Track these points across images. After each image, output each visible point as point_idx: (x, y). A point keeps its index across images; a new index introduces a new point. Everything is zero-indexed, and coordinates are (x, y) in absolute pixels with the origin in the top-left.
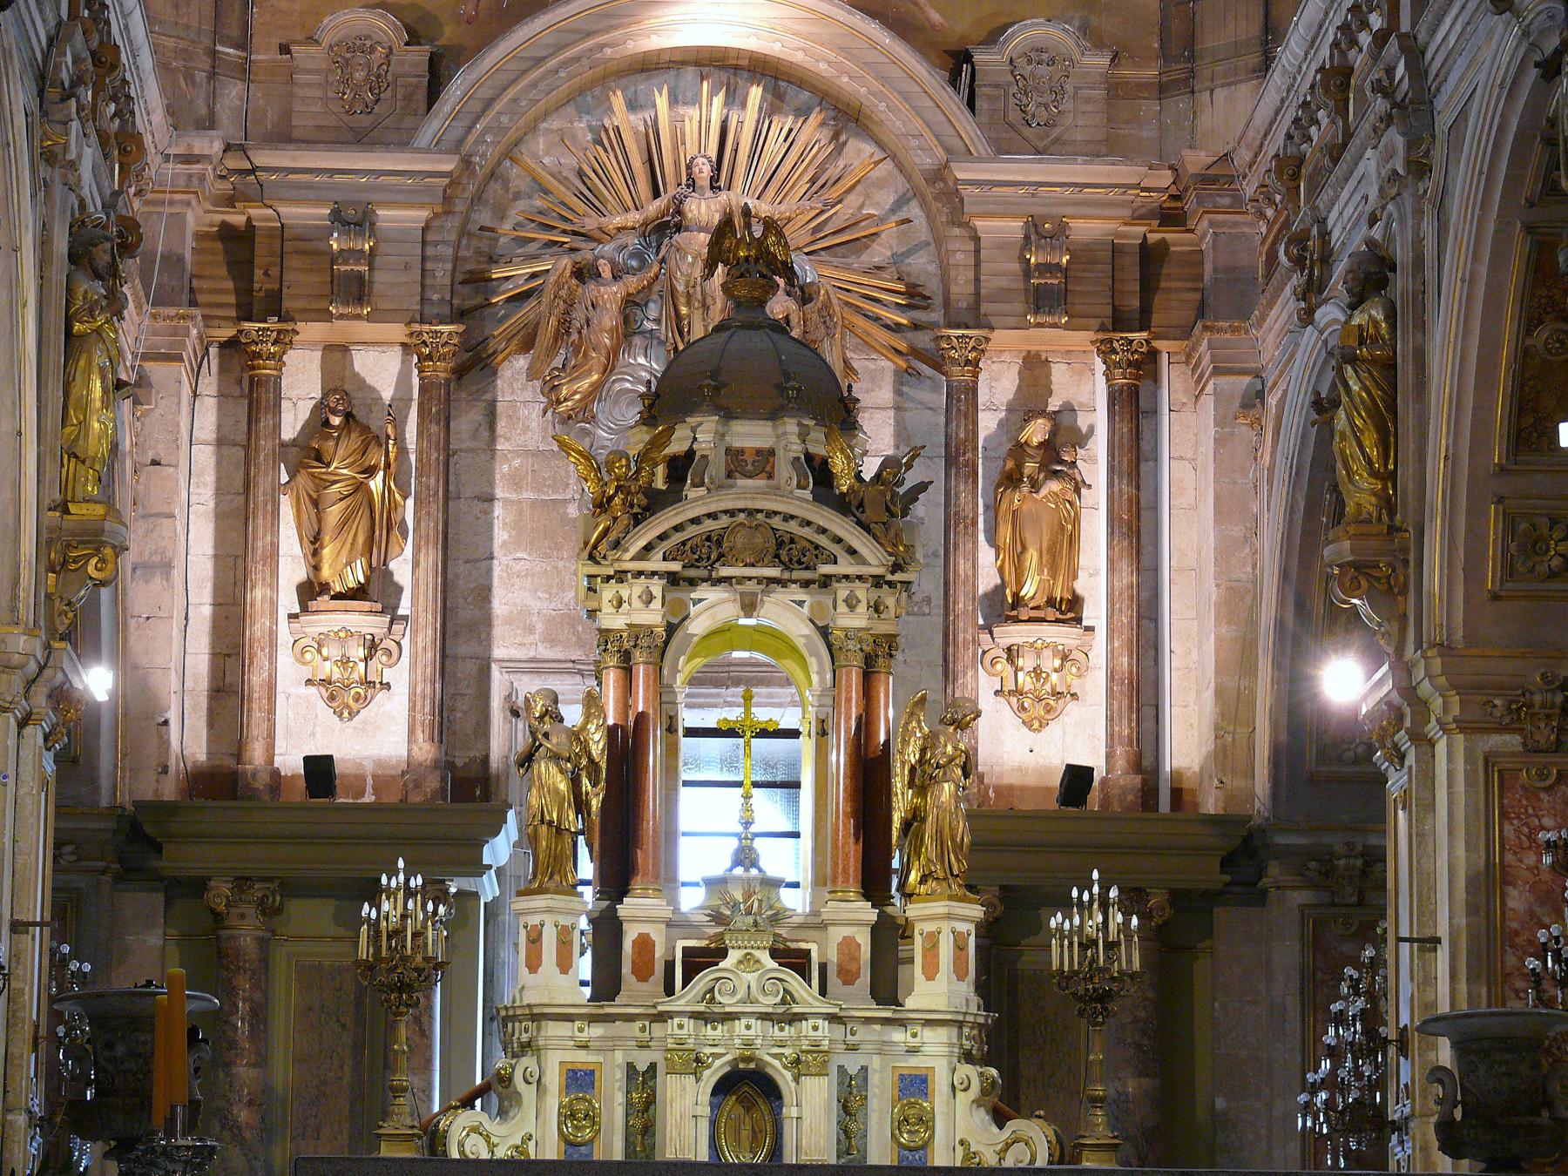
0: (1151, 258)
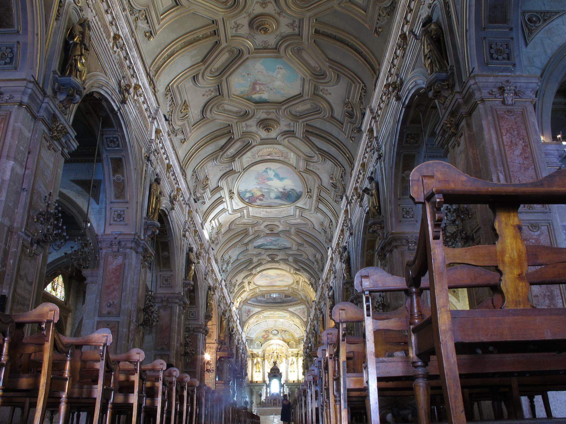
0: (298, 353)
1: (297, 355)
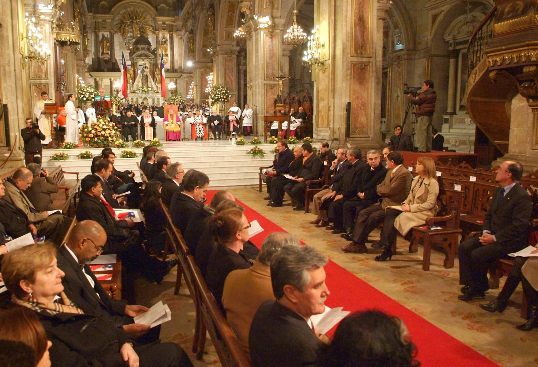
1: (171, 29)
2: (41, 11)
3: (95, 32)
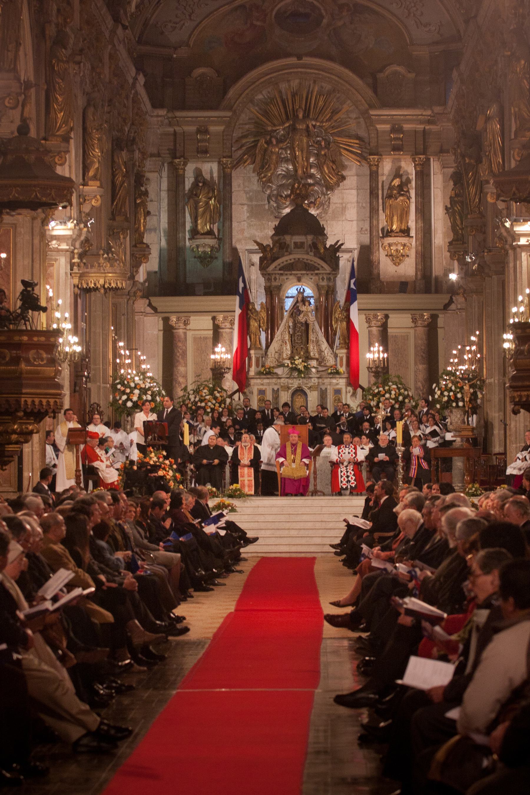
2: (55, 233)
3: (171, 164)
